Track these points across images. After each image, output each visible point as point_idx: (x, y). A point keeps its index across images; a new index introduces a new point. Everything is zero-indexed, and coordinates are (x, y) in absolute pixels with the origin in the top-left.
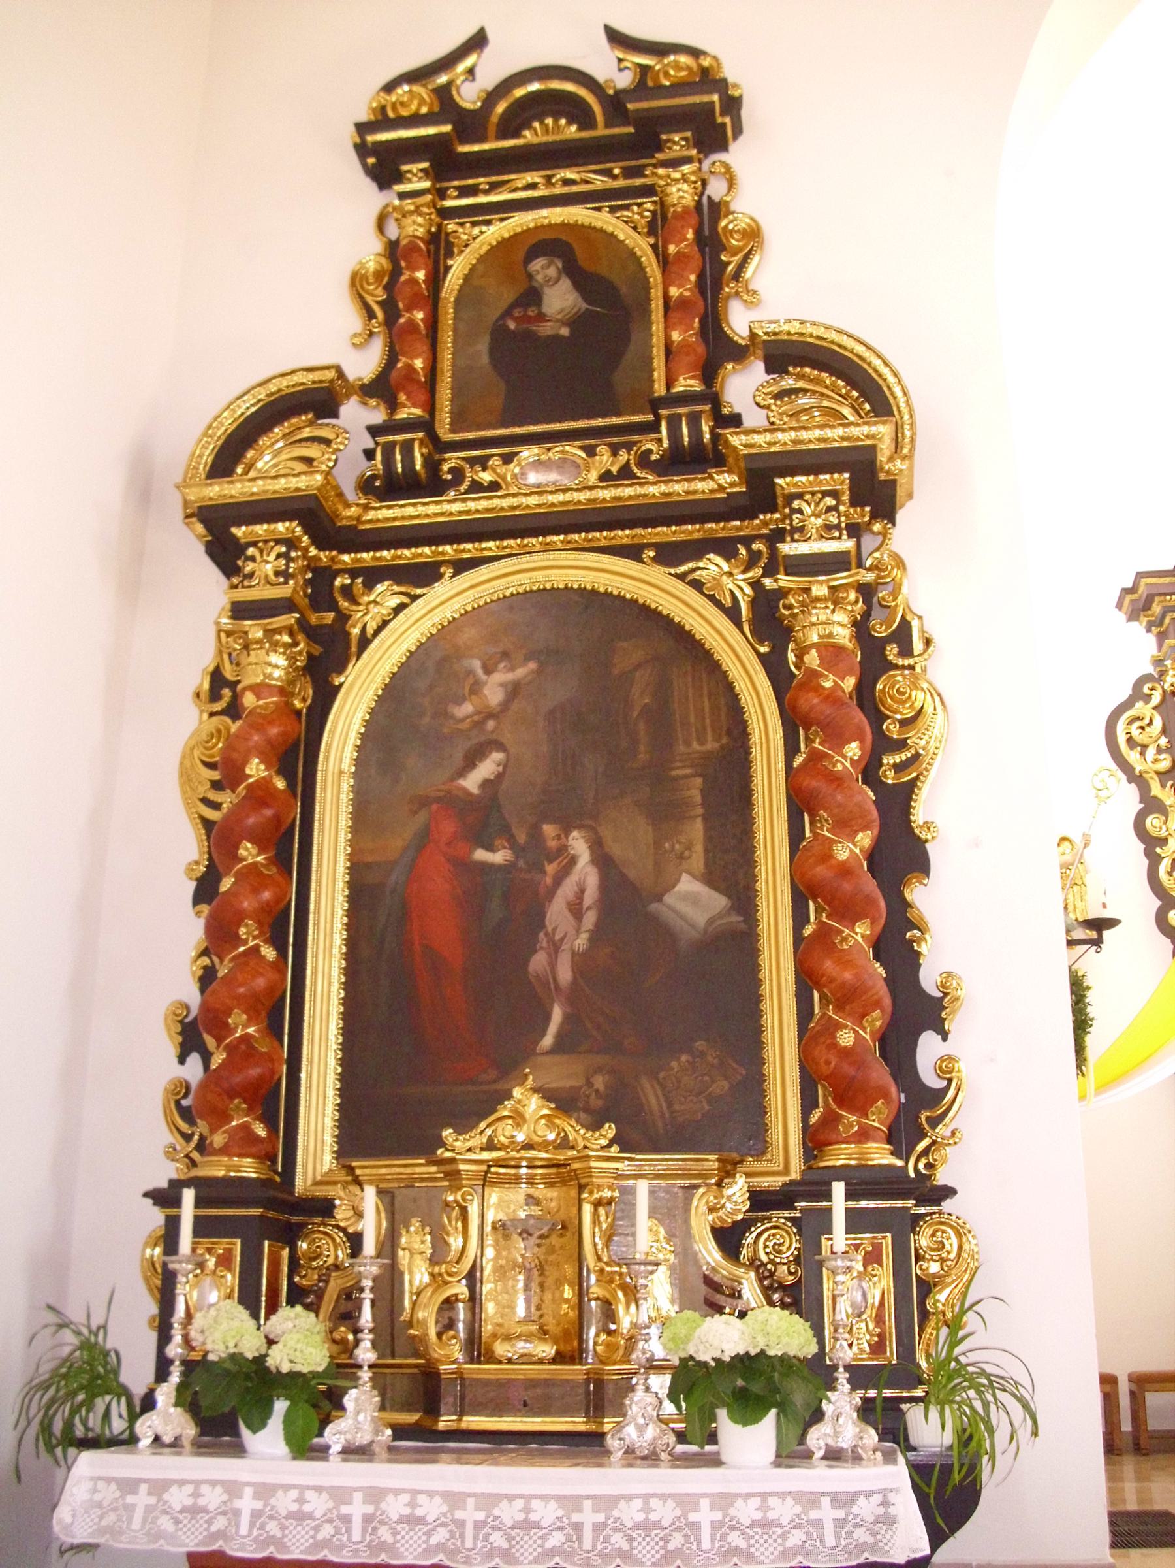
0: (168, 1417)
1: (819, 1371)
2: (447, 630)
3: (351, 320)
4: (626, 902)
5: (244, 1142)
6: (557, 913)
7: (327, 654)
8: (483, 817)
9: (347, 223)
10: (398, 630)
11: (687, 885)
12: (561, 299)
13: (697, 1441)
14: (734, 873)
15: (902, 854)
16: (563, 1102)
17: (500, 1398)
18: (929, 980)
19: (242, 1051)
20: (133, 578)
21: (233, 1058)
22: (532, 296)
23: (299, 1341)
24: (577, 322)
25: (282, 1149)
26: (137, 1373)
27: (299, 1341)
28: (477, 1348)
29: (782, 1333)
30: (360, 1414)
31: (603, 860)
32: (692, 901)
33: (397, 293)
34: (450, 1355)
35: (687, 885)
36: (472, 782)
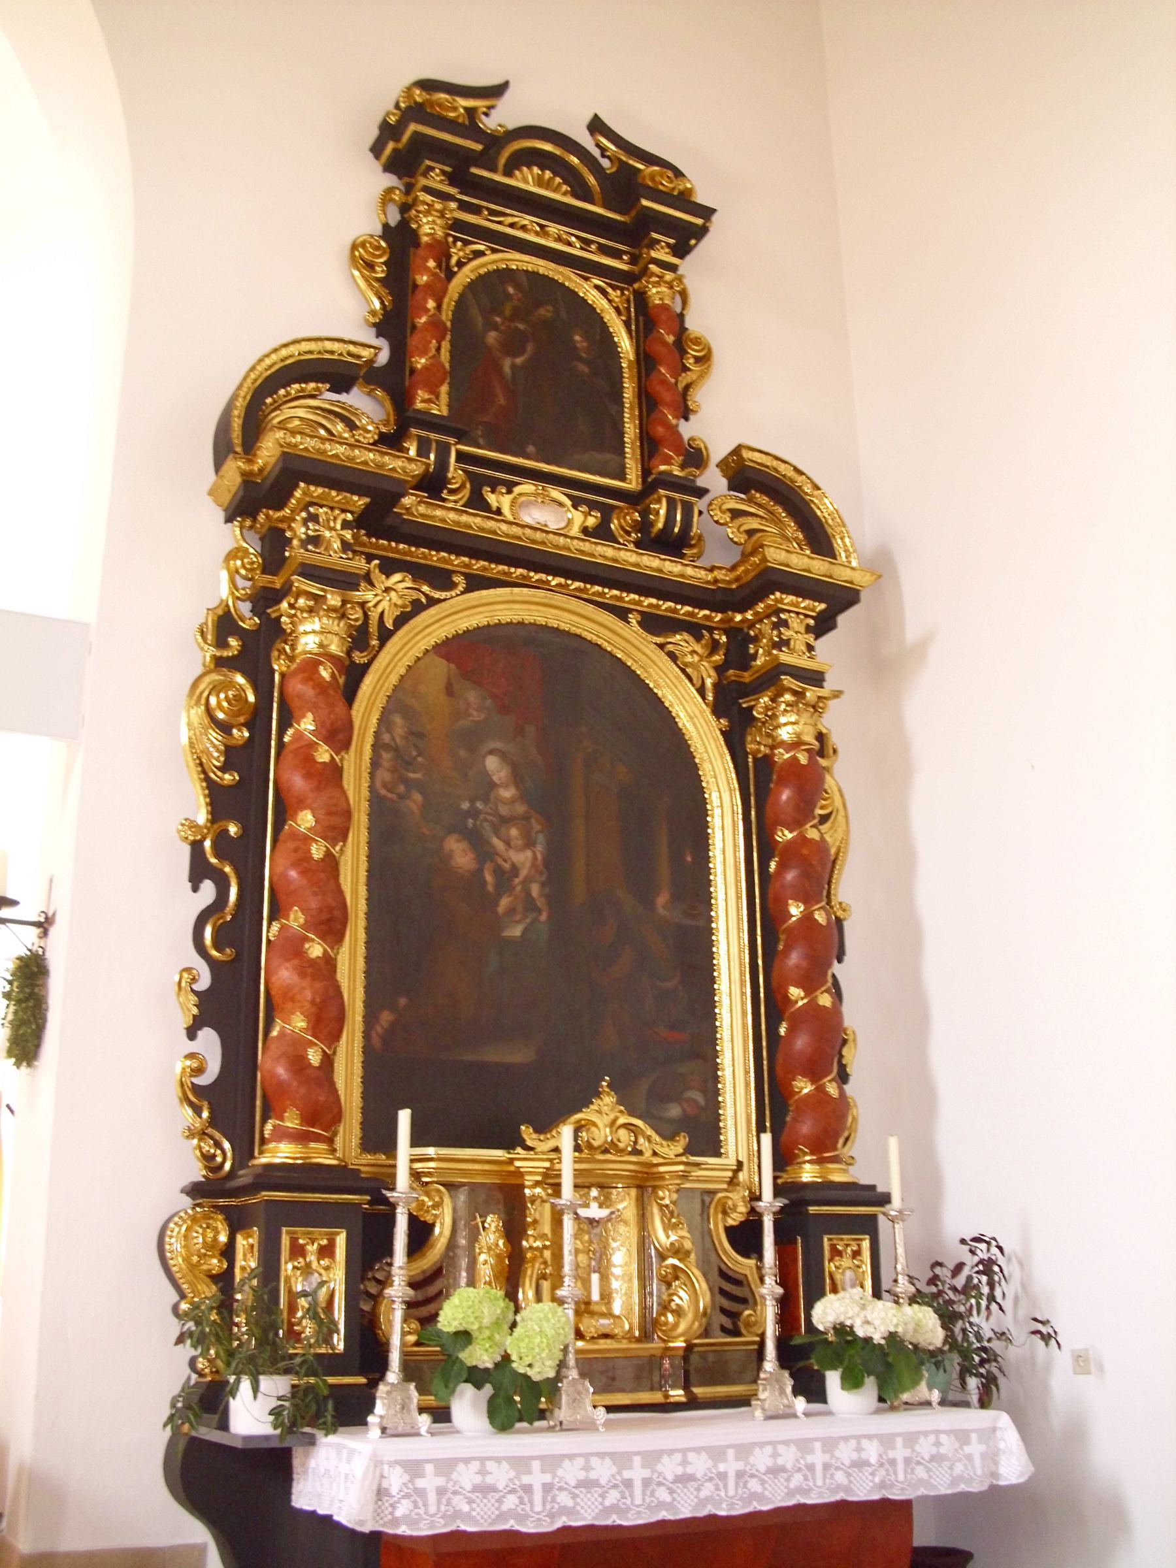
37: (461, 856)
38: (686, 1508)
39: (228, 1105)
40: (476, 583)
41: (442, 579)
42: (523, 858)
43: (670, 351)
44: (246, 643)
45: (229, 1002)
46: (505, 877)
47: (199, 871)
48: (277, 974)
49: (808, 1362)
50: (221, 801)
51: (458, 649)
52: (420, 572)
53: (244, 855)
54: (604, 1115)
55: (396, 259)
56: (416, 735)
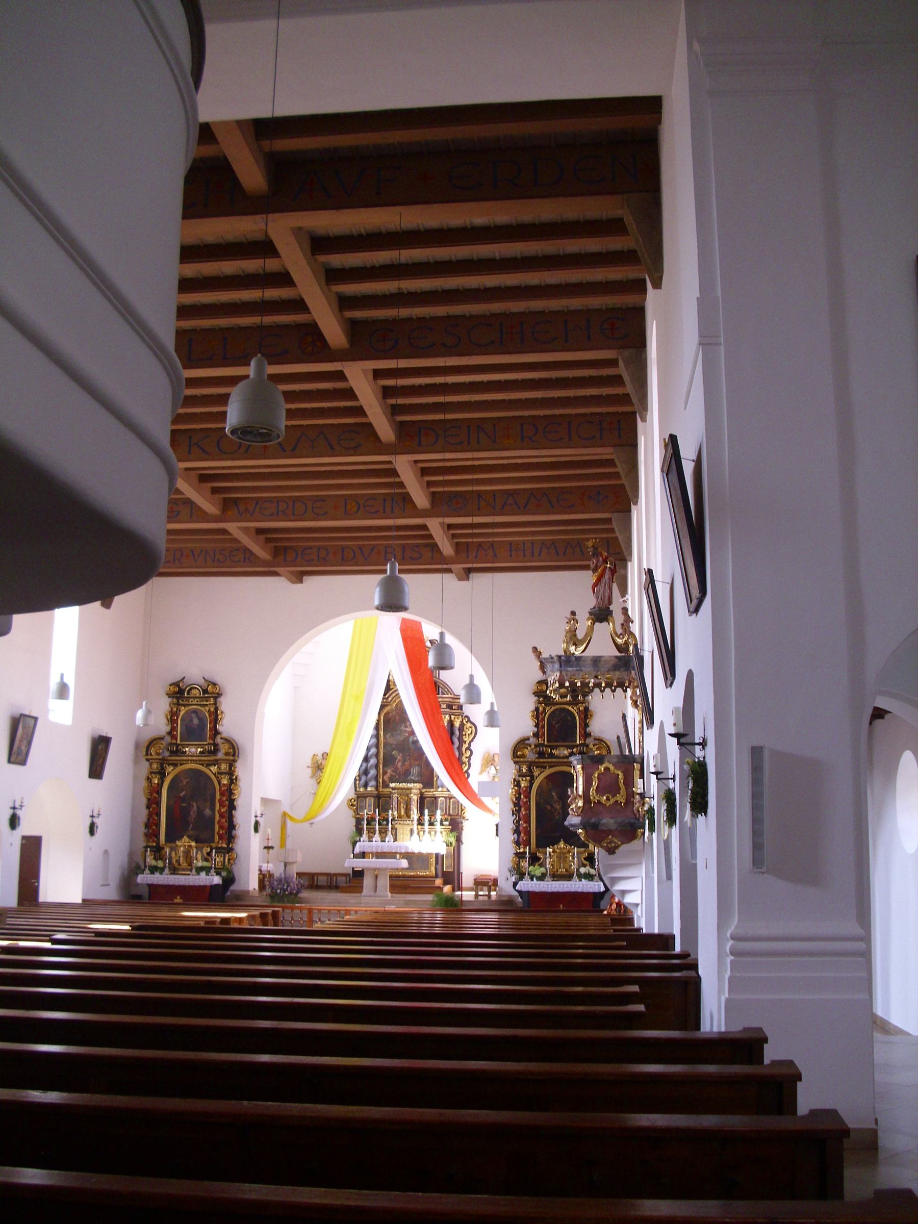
0: (147, 871)
1: (211, 868)
2: (179, 773)
3: (164, 721)
4: (200, 812)
5: (154, 841)
6: (192, 813)
7: (162, 774)
8: (183, 799)
9: (164, 704)
10: (171, 772)
11: (207, 810)
12: (196, 721)
13: (198, 874)
14: (213, 808)
15: (232, 807)
16: (189, 837)
17: (184, 870)
18: (235, 823)
19: (153, 830)
20: (136, 761)
21: (151, 826)
22: (191, 720)
23: (160, 864)
24: (198, 725)
25: (158, 842)
26: (143, 867)
27: (160, 864)
28: (179, 865)
29: (206, 864)
30: (167, 870)
31: (198, 807)
32: (208, 812)
33: (172, 718)
34: (176, 865)
35: (207, 810)
36: (182, 794)
37: (549, 807)
38: (556, 890)
39: (517, 843)
40: (550, 767)
41: (545, 768)
42: (558, 807)
43: (586, 714)
44: (517, 783)
45: (517, 831)
46: (555, 810)
47: (513, 814)
48: (521, 828)
49: (581, 876)
50: (515, 805)
51: (548, 777)
52: (541, 767)
53: (519, 811)
54: (562, 844)
55: (537, 714)
56: (542, 791)
